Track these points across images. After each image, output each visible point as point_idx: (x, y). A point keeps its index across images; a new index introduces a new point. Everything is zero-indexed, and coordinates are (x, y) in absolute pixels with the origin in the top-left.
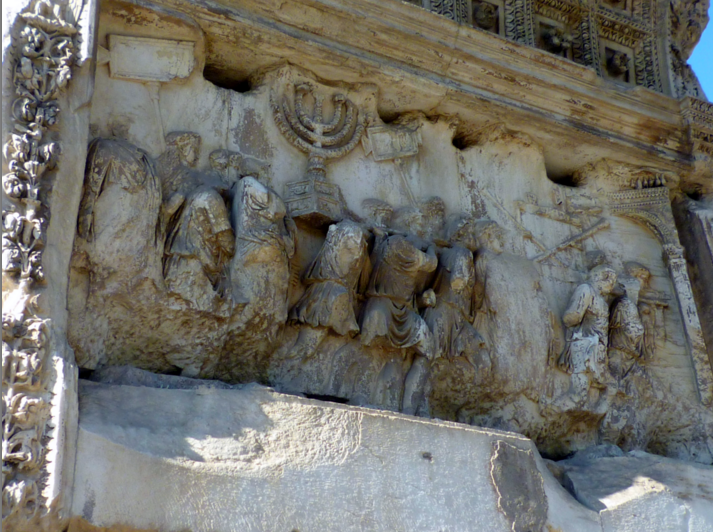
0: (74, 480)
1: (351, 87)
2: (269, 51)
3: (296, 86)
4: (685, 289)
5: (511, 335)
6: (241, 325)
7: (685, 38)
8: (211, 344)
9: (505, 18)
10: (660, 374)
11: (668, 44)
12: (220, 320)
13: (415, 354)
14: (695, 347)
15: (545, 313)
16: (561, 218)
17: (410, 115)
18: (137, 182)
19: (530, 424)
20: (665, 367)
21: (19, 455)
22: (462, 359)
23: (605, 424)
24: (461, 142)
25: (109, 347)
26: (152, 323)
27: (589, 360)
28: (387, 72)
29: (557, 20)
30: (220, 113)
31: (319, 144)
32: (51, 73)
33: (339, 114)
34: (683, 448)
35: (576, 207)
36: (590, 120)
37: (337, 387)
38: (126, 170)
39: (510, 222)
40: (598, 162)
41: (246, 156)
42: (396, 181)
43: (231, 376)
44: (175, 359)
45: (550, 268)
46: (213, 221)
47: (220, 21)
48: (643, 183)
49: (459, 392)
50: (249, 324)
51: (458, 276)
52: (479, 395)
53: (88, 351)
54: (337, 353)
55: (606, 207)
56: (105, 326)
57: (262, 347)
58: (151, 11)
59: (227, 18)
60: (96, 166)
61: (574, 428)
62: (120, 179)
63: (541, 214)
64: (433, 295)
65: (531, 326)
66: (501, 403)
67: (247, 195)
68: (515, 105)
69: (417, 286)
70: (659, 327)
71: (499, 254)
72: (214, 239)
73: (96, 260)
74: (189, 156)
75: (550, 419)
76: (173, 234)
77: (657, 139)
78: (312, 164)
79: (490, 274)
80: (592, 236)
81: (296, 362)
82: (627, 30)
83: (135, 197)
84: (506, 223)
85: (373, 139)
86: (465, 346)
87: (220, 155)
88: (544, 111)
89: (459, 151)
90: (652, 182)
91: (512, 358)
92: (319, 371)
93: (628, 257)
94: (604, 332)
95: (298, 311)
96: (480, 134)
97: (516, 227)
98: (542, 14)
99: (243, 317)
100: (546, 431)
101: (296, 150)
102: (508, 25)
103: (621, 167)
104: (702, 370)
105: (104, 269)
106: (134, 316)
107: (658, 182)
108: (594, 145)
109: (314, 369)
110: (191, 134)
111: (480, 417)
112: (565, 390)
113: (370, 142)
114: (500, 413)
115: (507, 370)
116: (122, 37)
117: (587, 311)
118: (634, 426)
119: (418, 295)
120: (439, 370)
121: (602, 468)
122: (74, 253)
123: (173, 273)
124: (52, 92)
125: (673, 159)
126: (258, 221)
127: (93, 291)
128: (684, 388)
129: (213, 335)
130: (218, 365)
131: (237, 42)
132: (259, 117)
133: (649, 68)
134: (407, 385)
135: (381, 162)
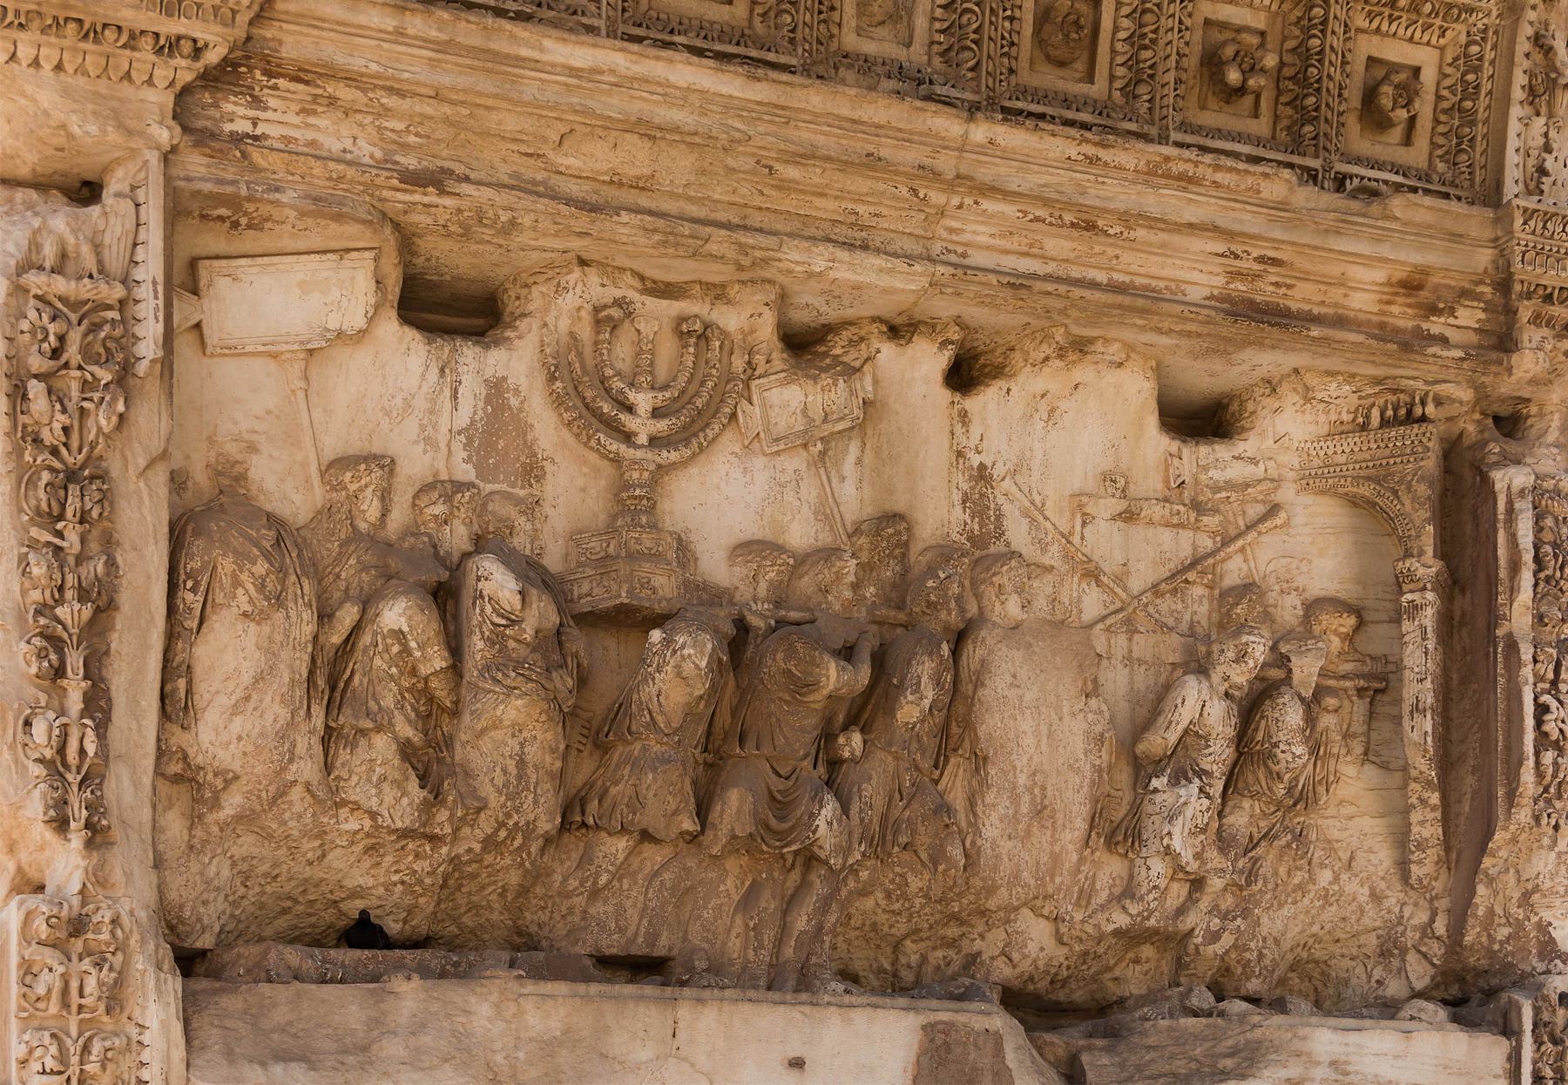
1: (718, 293)
2: (533, 243)
3: (596, 310)
5: (1015, 799)
9: (1116, 29)
13: (809, 859)
26: (310, 855)
28: (795, 256)
33: (689, 361)
37: (653, 938)
50: (489, 843)
51: (910, 698)
52: (938, 917)
53: (199, 920)
56: (226, 873)
57: (514, 878)
64: (857, 739)
65: (1059, 773)
69: (828, 721)
72: (420, 686)
73: (200, 760)
74: (370, 509)
76: (342, 685)
78: (627, 486)
81: (579, 901)
86: (914, 833)
90: (1403, 412)
91: (1010, 844)
92: (620, 912)
95: (583, 803)
102: (1119, 46)
104: (1422, 823)
106: (276, 849)
107: (1418, 411)
109: (610, 909)
110: (371, 459)
115: (995, 868)
116: (223, 263)
117: (1186, 731)
118: (1252, 945)
119: (827, 737)
122: (161, 753)
123: (343, 765)
129: (422, 866)
131: (466, 234)
133: (1468, 104)
134: (789, 919)
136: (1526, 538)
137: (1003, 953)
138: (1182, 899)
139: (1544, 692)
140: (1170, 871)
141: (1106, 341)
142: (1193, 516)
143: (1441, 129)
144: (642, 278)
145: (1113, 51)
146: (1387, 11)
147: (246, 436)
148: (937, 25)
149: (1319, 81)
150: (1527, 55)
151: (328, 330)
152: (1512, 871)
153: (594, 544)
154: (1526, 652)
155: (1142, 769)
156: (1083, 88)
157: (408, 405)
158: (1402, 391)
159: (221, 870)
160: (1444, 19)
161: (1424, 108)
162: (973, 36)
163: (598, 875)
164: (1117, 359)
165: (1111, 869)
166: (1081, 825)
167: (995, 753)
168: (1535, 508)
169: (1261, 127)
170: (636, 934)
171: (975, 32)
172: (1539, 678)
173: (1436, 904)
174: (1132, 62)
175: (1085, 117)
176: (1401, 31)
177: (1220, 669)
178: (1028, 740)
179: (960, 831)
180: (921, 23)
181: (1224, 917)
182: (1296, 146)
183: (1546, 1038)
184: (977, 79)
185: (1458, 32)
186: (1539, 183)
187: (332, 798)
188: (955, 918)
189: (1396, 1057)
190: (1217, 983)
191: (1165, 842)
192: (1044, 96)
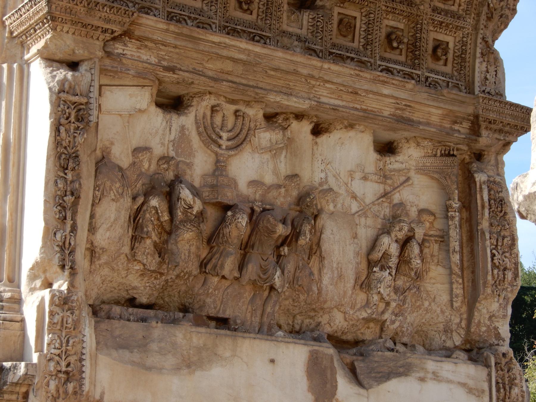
0: (95, 381)
1: (248, 104)
4: (454, 234)
5: (333, 272)
6: (173, 277)
7: (496, 27)
8: (155, 287)
9: (361, 28)
10: (429, 289)
11: (480, 36)
12: (162, 274)
13: (272, 288)
14: (454, 274)
15: (358, 254)
16: (379, 181)
17: (285, 115)
18: (119, 195)
19: (338, 326)
20: (434, 284)
21: (70, 369)
22: (300, 288)
23: (386, 326)
24: (317, 131)
25: (99, 290)
27: (380, 287)
29: (399, 22)
30: (165, 129)
31: (224, 147)
32: (75, 134)
34: (437, 336)
35: (391, 171)
38: (113, 188)
39: (343, 188)
41: (179, 159)
42: (271, 166)
43: (164, 301)
44: (133, 293)
45: (366, 219)
46: (160, 214)
47: (169, 75)
48: (441, 151)
49: (296, 307)
54: (226, 290)
55: (413, 168)
56: (99, 280)
57: (183, 288)
58: (128, 74)
59: (174, 73)
60: (97, 186)
61: (366, 325)
62: (110, 193)
63: (365, 178)
64: (286, 249)
66: (321, 314)
67: (181, 199)
68: (356, 109)
70: (434, 256)
71: (332, 213)
74: (146, 165)
75: (351, 323)
76: (136, 221)
77: (455, 122)
79: (324, 231)
80: (399, 191)
82: (451, 26)
83: (118, 204)
84: (340, 188)
85: (258, 138)
87: (164, 161)
88: (376, 110)
89: (314, 137)
90: (447, 152)
91: (331, 287)
92: (214, 301)
93: (423, 205)
94: (394, 266)
96: (331, 124)
97: (347, 191)
98: (388, 19)
99: (174, 272)
100: (348, 329)
101: (209, 152)
102: (362, 33)
103: (426, 142)
104: (456, 288)
105: (100, 249)
107: (452, 153)
108: (408, 131)
109: (211, 300)
111: (308, 320)
112: (363, 304)
113: (257, 139)
114: (320, 319)
115: (327, 295)
116: (109, 87)
117: (384, 253)
118: (405, 326)
119: (278, 247)
120: (285, 295)
124: (76, 147)
125: (464, 136)
126: (186, 215)
127: (94, 262)
128: (445, 298)
130: (157, 297)
132: (188, 130)
133: (463, 56)
135: (262, 153)
137: (328, 323)
138: (383, 309)
139: (494, 249)
141: (359, 125)
142: (384, 179)
143: (455, 62)
144: (226, 98)
145: (360, 35)
146: (439, 26)
147: (111, 140)
148: (310, 24)
149: (420, 47)
150: (481, 43)
151: (136, 108)
153: (209, 180)
155: (371, 264)
156: (351, 44)
157: (157, 132)
159: (98, 280)
160: (456, 29)
161: (450, 56)
162: (321, 29)
163: (209, 289)
165: (361, 297)
166: (352, 282)
168: (488, 187)
169: (402, 58)
170: (219, 310)
171: (321, 28)
173: (462, 316)
174: (366, 38)
175: (352, 55)
176: (443, 32)
177: (394, 233)
178: (336, 252)
179: (316, 281)
180: (305, 22)
181: (396, 315)
182: (413, 67)
184: (322, 42)
185: (460, 34)
186: (485, 82)
187: (132, 257)
188: (314, 310)
190: (393, 337)
192: (340, 48)
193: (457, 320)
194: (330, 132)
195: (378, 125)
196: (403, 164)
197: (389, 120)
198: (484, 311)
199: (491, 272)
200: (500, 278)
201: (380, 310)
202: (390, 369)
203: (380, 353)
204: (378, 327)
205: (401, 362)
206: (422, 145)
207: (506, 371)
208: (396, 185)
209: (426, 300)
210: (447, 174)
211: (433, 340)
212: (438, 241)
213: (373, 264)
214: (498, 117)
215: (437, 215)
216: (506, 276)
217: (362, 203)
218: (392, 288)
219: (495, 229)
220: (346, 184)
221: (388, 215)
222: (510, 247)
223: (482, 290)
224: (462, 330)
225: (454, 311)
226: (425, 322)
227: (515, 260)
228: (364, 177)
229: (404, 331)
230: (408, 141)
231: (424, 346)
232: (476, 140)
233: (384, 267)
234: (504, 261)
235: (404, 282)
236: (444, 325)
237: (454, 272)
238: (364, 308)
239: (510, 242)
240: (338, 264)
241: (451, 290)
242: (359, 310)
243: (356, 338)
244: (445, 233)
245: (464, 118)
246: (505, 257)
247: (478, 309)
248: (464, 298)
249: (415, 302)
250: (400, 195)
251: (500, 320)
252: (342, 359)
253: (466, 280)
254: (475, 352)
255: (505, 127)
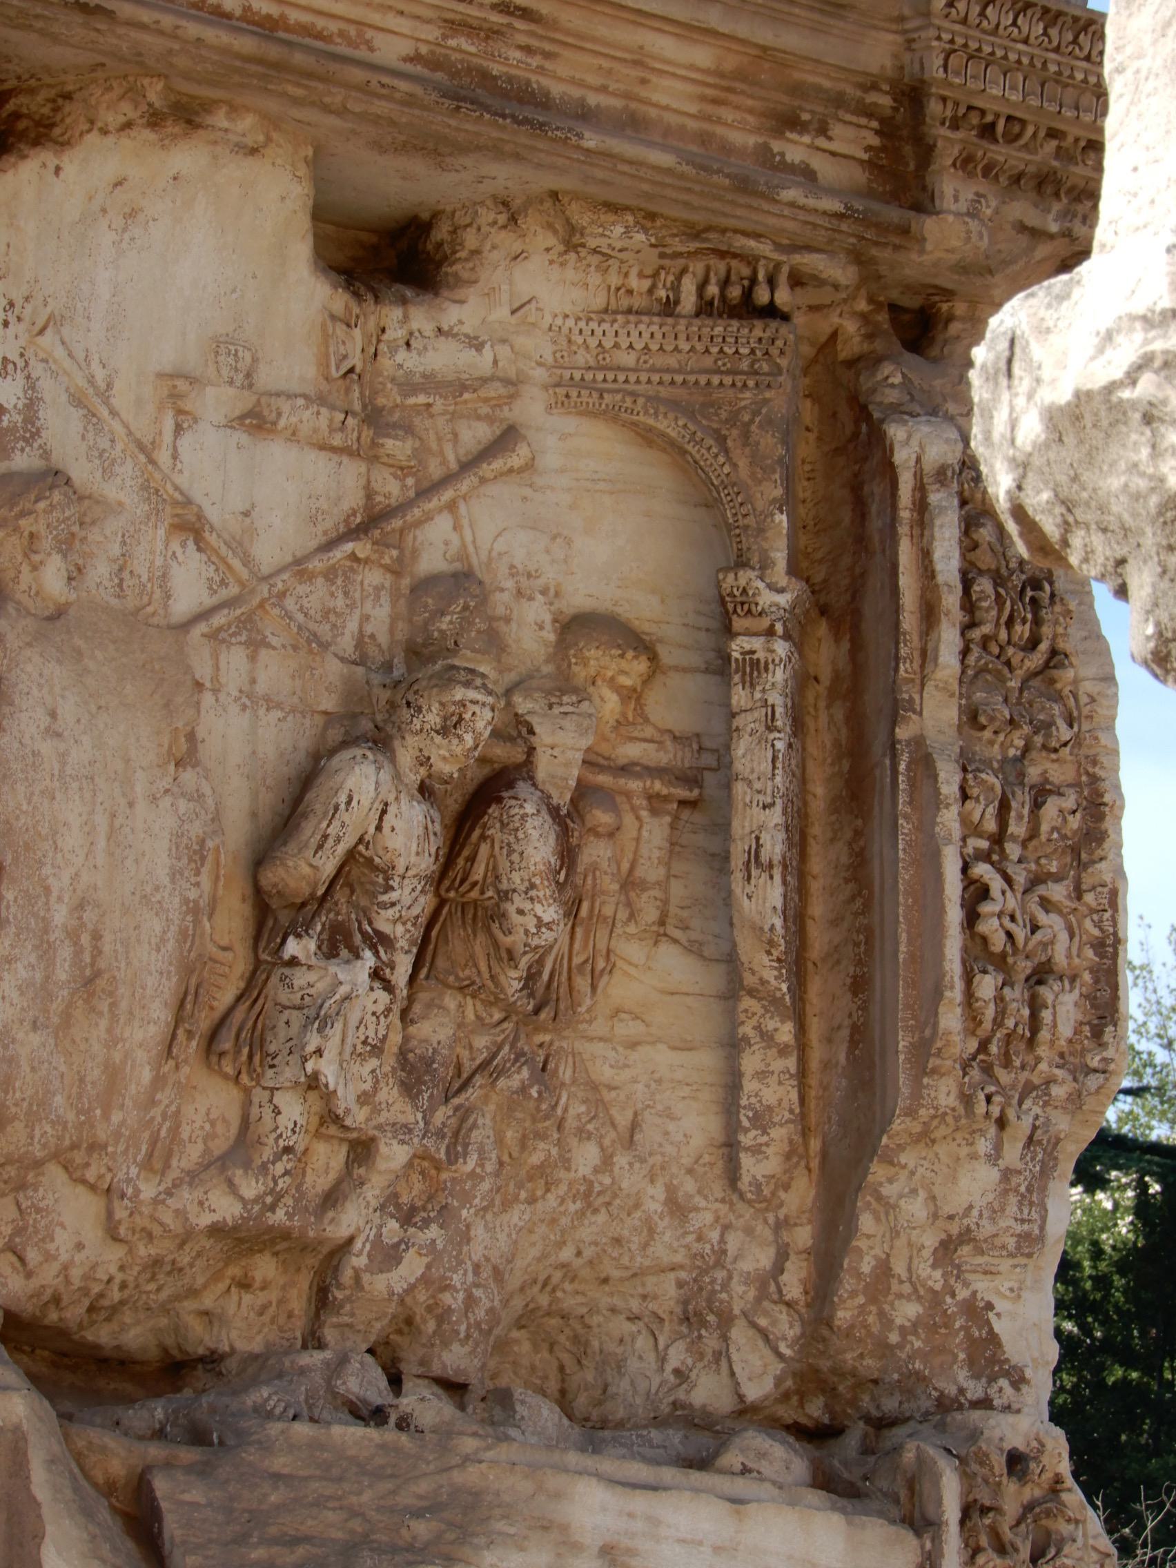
5: (46, 951)
10: (605, 1073)
14: (751, 993)
16: (337, 440)
19: (65, 1268)
20: (633, 1045)
23: (347, 1276)
27: (319, 1052)
34: (643, 1342)
35: (409, 386)
36: (518, 54)
39: (127, 470)
40: (529, 202)
45: (253, 658)
48: (701, 288)
55: (540, 374)
61: (234, 1271)
70: (643, 886)
71: (58, 614)
75: (144, 1251)
77: (789, 122)
80: (452, 507)
84: (108, 472)
88: (333, 27)
90: (735, 292)
91: (36, 1039)
94: (403, 935)
96: (68, 96)
97: (149, 490)
100: (123, 1286)
104: (761, 1075)
107: (762, 296)
108: (517, 157)
112: (220, 1146)
117: (351, 855)
118: (456, 1279)
121: (280, 1463)
125: (836, 206)
136: (947, 561)
138: (332, 1176)
139: (985, 857)
140: (315, 1120)
141: (234, 110)
142: (367, 434)
152: (922, 1194)
154: (949, 780)
158: (735, 256)
164: (249, 141)
166: (160, 1013)
167: (16, 859)
168: (963, 503)
172: (971, 829)
173: (785, 1236)
177: (411, 740)
178: (72, 840)
181: (407, 1218)
183: (984, 1541)
189: (717, 1550)
191: (310, 1066)
193: (762, 1258)
194: (64, 145)
195: (342, 112)
196: (479, 348)
197: (404, 86)
198: (916, 1208)
199: (959, 985)
200: (1010, 1023)
201: (318, 1181)
202: (356, 1525)
203: (302, 1430)
204: (304, 1282)
205: (423, 1487)
206: (592, 243)
207: (1025, 1552)
208: (435, 470)
209: (583, 1134)
210: (733, 420)
211: (620, 1366)
212: (666, 799)
213: (284, 918)
214: (1034, 102)
215: (667, 655)
216: (1046, 1015)
217: (236, 563)
218: (390, 1061)
219: (992, 747)
220: (141, 447)
221: (383, 639)
222: (1075, 851)
223: (905, 1091)
224: (783, 1316)
225: (740, 1206)
226: (578, 1262)
227: (1098, 925)
228: (250, 414)
229: (449, 1310)
230: (513, 219)
231: (564, 1401)
232: (905, 231)
233: (348, 937)
234: (1035, 928)
235: (460, 1026)
236: (680, 1284)
237: (749, 980)
238: (223, 1169)
239: (1075, 822)
240: (81, 906)
241: (732, 1084)
242: (193, 1177)
243: (170, 1341)
244: (708, 760)
245: (839, 101)
246: (1046, 904)
247: (879, 1198)
248: (805, 1132)
249: (523, 1146)
250: (457, 527)
251: (1005, 1265)
252: (78, 1457)
253: (816, 1029)
254: (852, 1441)
255: (1071, 159)
